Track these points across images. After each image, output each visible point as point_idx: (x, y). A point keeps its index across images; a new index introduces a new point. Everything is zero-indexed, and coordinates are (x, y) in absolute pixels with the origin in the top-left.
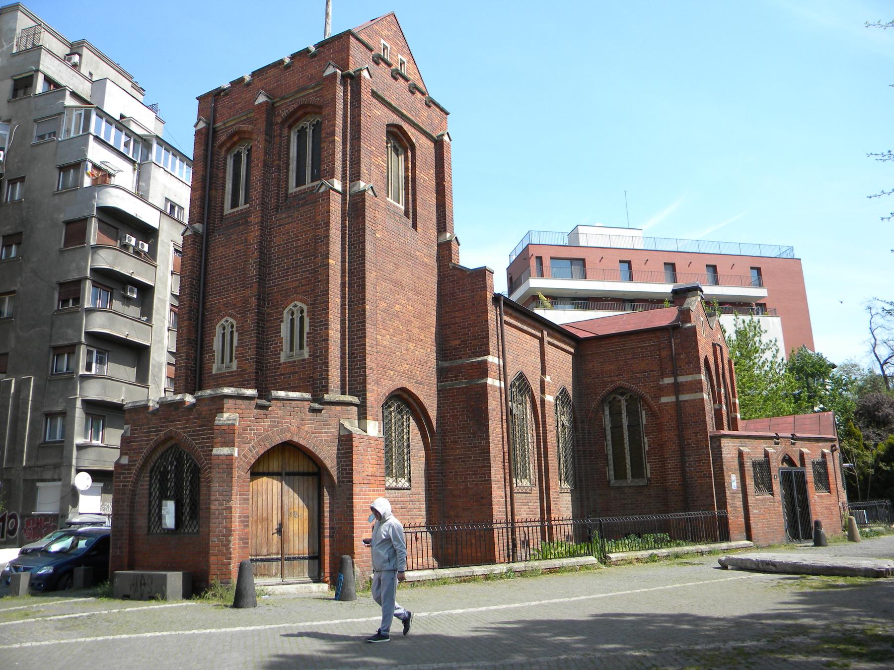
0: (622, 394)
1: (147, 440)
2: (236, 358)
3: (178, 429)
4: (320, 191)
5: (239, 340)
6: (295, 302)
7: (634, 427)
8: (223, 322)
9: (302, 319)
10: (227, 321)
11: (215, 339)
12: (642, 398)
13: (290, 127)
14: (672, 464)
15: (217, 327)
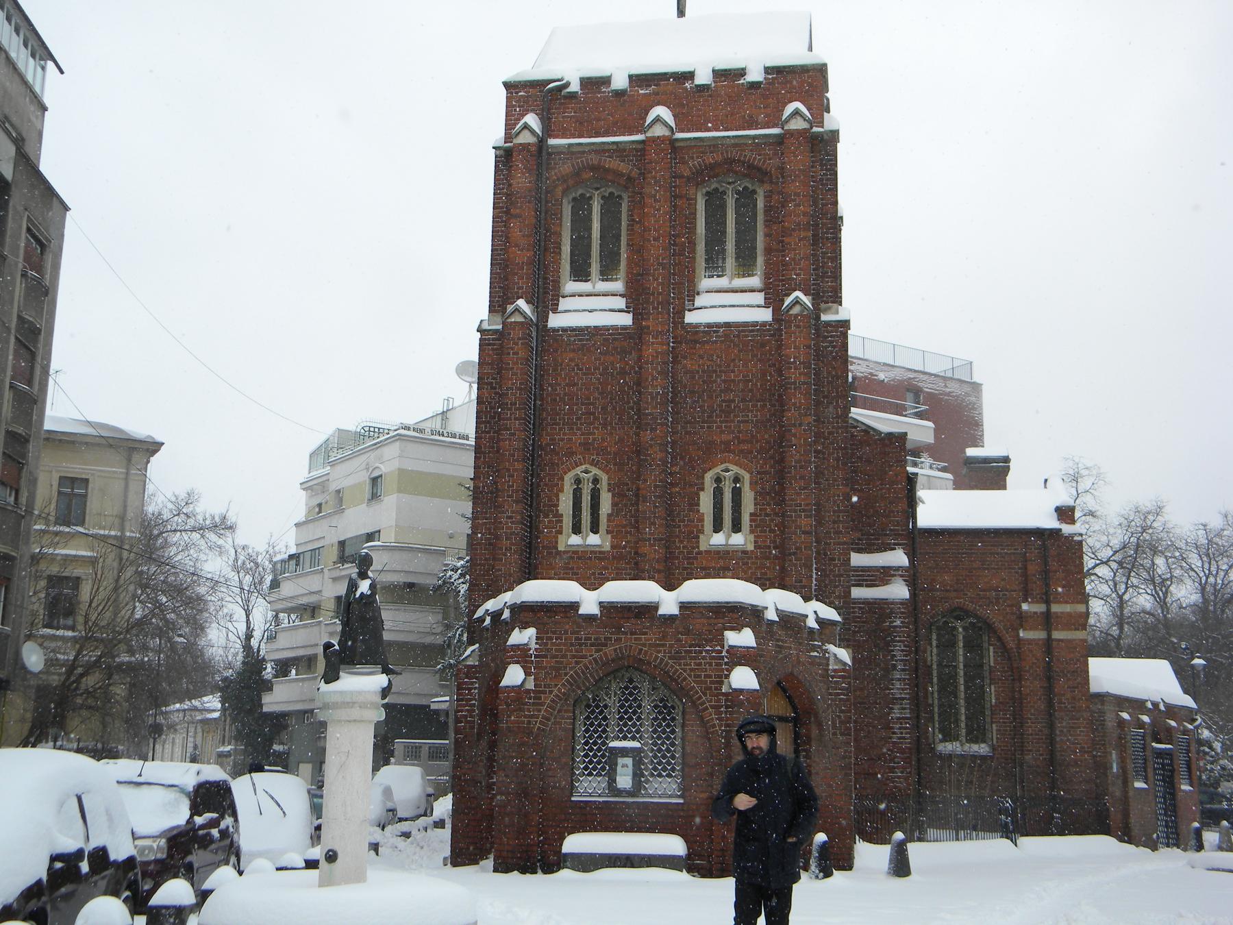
0: (958, 618)
1: (574, 657)
2: (608, 532)
3: (644, 645)
4: (791, 312)
5: (614, 504)
6: (727, 464)
7: (975, 669)
8: (578, 470)
9: (737, 493)
10: (586, 472)
11: (561, 495)
12: (990, 627)
13: (697, 185)
14: (1034, 726)
15: (568, 478)
